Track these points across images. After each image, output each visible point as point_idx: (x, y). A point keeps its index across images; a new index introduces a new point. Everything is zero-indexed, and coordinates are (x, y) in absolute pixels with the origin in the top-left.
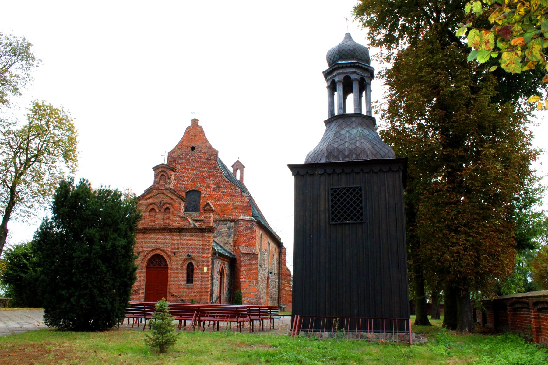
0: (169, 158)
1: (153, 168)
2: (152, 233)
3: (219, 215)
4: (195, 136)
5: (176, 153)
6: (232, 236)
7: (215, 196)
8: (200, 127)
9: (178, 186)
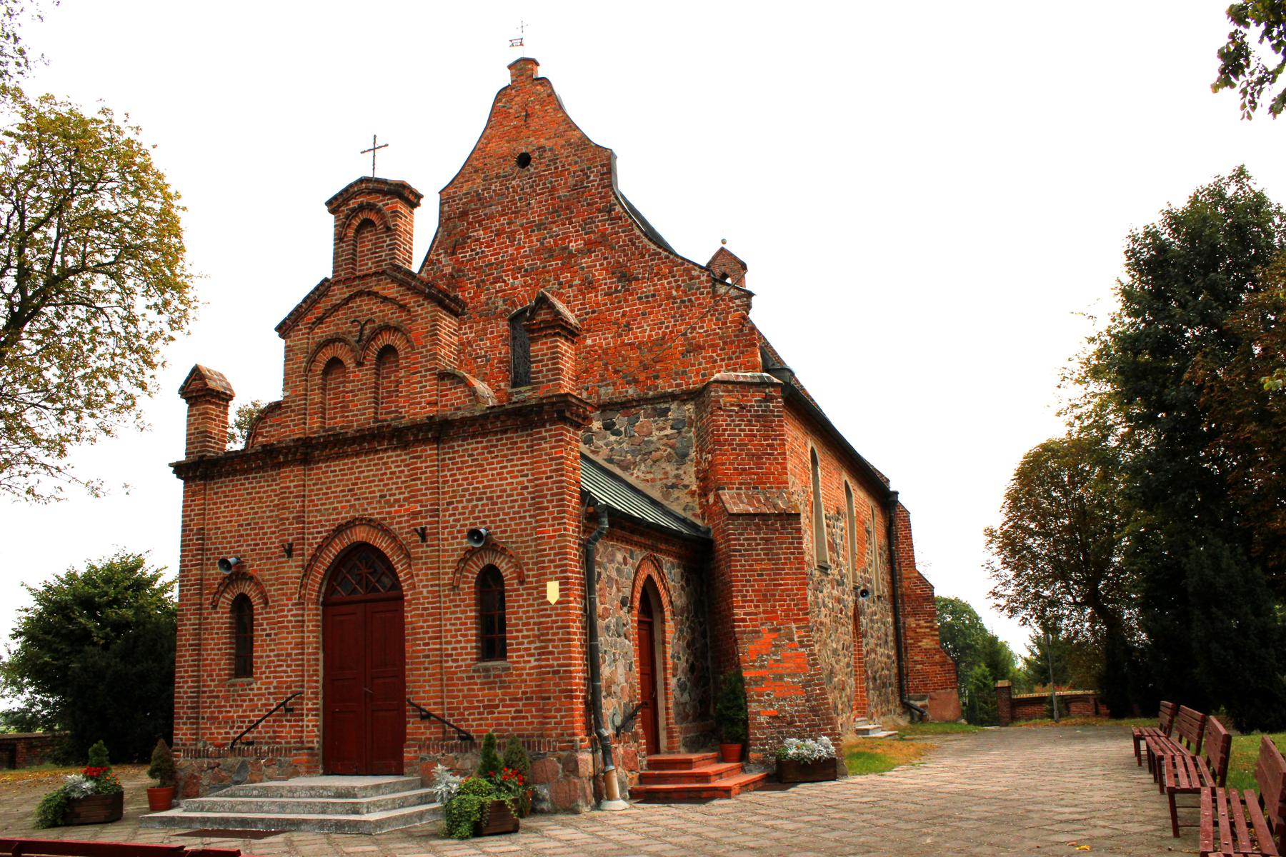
0: (446, 208)
1: (329, 203)
2: (334, 459)
3: (636, 381)
4: (527, 116)
5: (465, 188)
6: (693, 454)
7: (617, 314)
8: (544, 82)
9: (483, 298)
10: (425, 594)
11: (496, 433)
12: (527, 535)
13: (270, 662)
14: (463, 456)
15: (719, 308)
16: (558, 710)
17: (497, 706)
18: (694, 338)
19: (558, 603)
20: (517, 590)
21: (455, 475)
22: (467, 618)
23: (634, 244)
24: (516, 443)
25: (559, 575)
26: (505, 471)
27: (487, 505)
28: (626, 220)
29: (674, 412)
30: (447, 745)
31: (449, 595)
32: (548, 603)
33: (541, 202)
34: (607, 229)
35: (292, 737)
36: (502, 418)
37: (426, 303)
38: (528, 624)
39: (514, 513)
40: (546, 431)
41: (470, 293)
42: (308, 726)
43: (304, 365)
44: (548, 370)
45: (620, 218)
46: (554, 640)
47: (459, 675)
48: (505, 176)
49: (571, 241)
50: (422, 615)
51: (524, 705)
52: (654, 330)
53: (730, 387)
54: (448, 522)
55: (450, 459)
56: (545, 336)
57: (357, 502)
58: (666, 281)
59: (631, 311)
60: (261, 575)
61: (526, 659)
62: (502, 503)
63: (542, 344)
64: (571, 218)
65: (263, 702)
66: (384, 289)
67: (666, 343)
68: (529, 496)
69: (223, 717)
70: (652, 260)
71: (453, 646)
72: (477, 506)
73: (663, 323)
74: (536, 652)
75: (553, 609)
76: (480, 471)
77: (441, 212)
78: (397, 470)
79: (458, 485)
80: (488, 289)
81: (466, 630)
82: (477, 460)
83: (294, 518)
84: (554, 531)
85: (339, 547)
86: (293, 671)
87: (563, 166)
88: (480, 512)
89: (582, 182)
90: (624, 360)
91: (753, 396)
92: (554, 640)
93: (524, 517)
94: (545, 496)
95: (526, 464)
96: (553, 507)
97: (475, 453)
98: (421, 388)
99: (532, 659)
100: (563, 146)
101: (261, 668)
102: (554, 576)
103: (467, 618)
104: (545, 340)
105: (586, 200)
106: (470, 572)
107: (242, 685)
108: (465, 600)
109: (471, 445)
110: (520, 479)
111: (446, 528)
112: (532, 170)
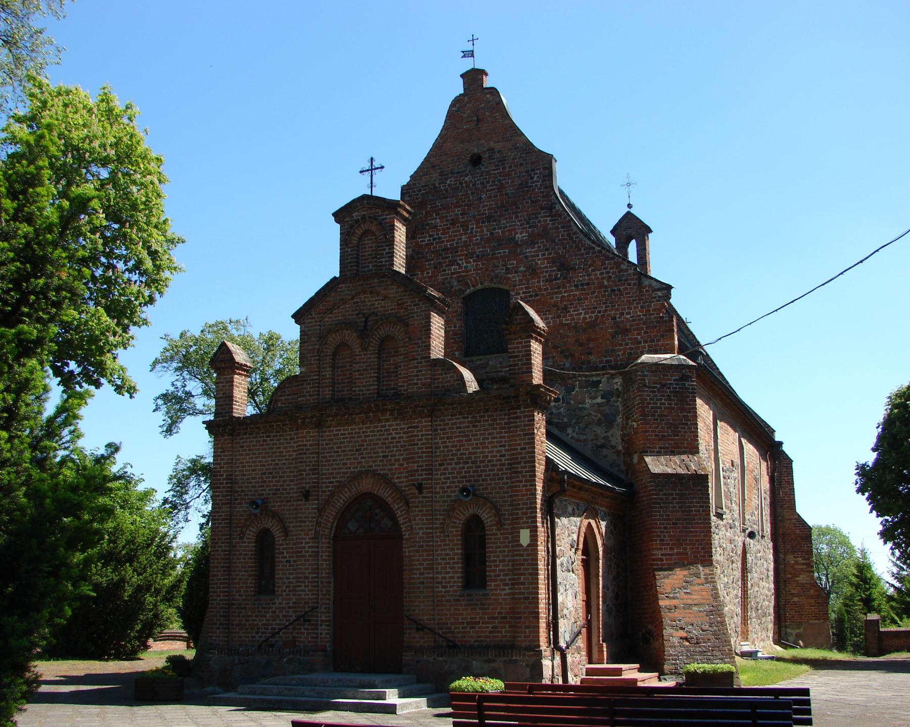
1: (334, 215)
4: (478, 120)
6: (619, 420)
7: (556, 298)
8: (494, 91)
10: (421, 535)
13: (289, 583)
18: (622, 322)
19: (529, 546)
21: (445, 442)
22: (454, 554)
23: (571, 238)
27: (472, 467)
28: (565, 218)
31: (440, 536)
32: (521, 546)
41: (428, 273)
47: (448, 598)
49: (517, 233)
50: (418, 551)
51: (499, 623)
55: (441, 430)
57: (363, 460)
58: (599, 272)
62: (484, 466)
70: (587, 253)
71: (443, 575)
81: (454, 563)
84: (527, 490)
86: (309, 590)
88: (466, 472)
91: (672, 376)
92: (524, 574)
93: (502, 479)
95: (504, 437)
97: (462, 426)
98: (417, 371)
99: (507, 588)
102: (526, 525)
103: (454, 554)
112: (483, 169)
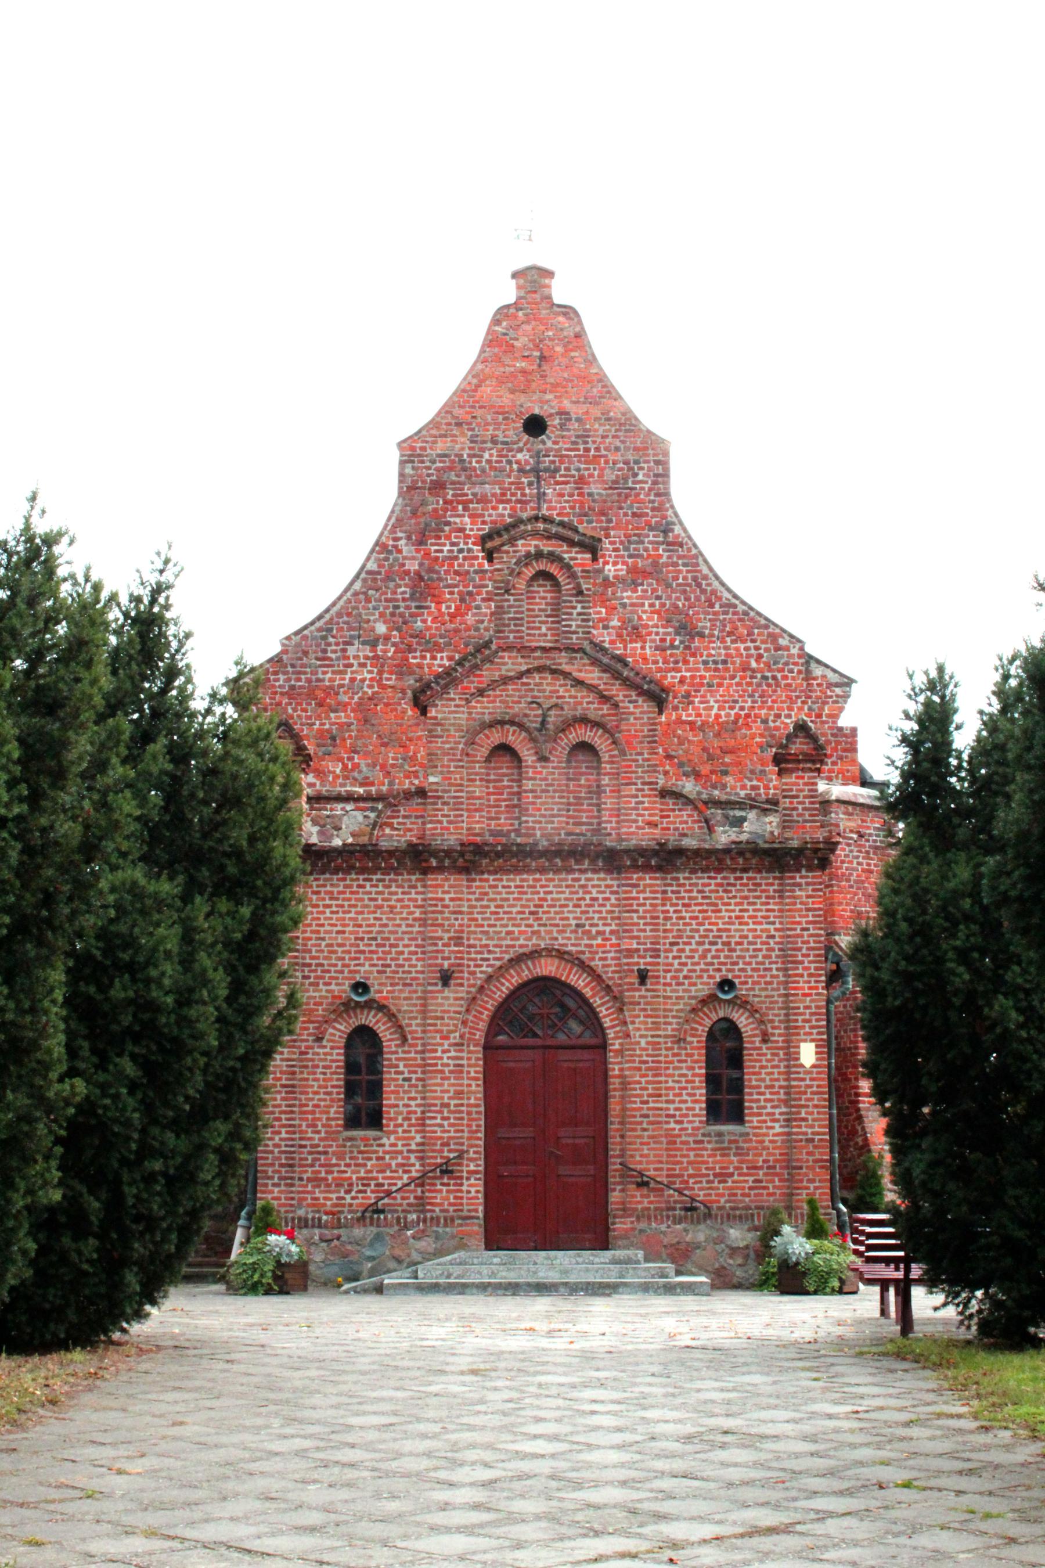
0: (408, 470)
2: (507, 872)
3: (697, 776)
4: (543, 358)
5: (441, 447)
8: (569, 312)
9: (470, 619)
10: (643, 1044)
11: (734, 870)
12: (773, 989)
13: (409, 1113)
14: (691, 891)
15: (813, 695)
16: (813, 1181)
17: (732, 1175)
18: (777, 728)
19: (814, 1066)
20: (760, 1048)
21: (680, 911)
22: (694, 1075)
23: (699, 585)
24: (760, 885)
25: (815, 1037)
26: (746, 914)
27: (722, 951)
28: (689, 550)
29: (752, 823)
30: (674, 1216)
31: (672, 1048)
32: (802, 1066)
33: (562, 495)
34: (661, 556)
35: (450, 1204)
36: (748, 855)
37: (640, 700)
38: (773, 1087)
39: (757, 963)
40: (801, 877)
41: (448, 607)
42: (469, 1192)
43: (461, 746)
44: (804, 809)
45: (681, 545)
46: (807, 1106)
47: (684, 1138)
48: (506, 443)
49: (607, 563)
50: (639, 1069)
51: (765, 1174)
52: (724, 709)
53: (850, 808)
54: (672, 965)
55: (673, 892)
56: (803, 770)
57: (542, 929)
58: (742, 646)
59: (693, 677)
60: (395, 1005)
61: (769, 1124)
62: (742, 950)
63: (797, 777)
64: (607, 529)
65: (400, 1160)
66: (580, 671)
67: (740, 729)
68: (777, 947)
69: (334, 1179)
70: (726, 613)
71: (677, 1105)
72: (710, 950)
73: (736, 702)
74: (782, 1117)
75: (807, 1072)
76: (713, 911)
77: (402, 475)
78: (600, 896)
79: (685, 924)
80: (478, 607)
81: (693, 1088)
82: (709, 898)
83: (450, 939)
84: (810, 988)
85: (516, 980)
86: (450, 1125)
87: (597, 449)
88: (713, 957)
89: (625, 479)
90: (681, 743)
91: (872, 821)
92: (807, 1106)
93: (770, 969)
94: (800, 949)
95: (773, 910)
96: (810, 962)
97: (707, 889)
98: (637, 803)
99: (777, 1125)
100: (596, 419)
101: (396, 1119)
102: (809, 1038)
103: (694, 1075)
104: (800, 774)
105: (631, 507)
106: (701, 1024)
107: (365, 1139)
108: (692, 1055)
109: (701, 880)
110: (765, 926)
111: (669, 971)
112: (549, 444)
